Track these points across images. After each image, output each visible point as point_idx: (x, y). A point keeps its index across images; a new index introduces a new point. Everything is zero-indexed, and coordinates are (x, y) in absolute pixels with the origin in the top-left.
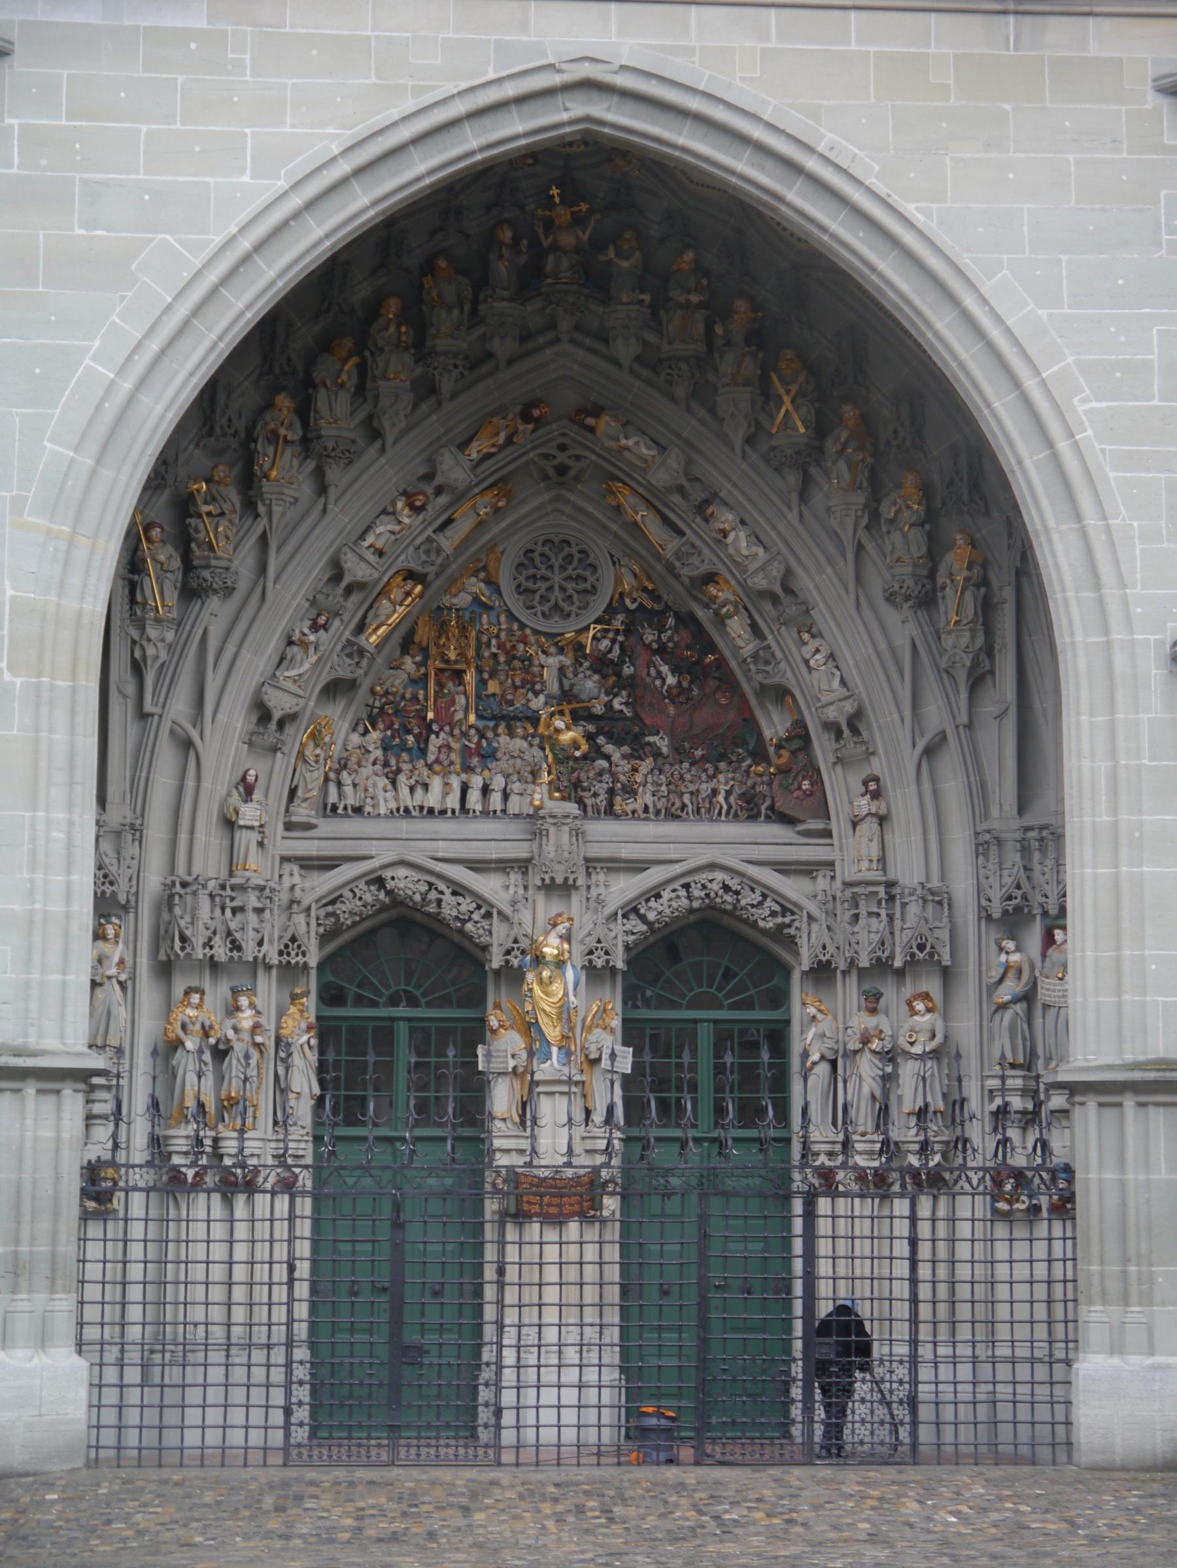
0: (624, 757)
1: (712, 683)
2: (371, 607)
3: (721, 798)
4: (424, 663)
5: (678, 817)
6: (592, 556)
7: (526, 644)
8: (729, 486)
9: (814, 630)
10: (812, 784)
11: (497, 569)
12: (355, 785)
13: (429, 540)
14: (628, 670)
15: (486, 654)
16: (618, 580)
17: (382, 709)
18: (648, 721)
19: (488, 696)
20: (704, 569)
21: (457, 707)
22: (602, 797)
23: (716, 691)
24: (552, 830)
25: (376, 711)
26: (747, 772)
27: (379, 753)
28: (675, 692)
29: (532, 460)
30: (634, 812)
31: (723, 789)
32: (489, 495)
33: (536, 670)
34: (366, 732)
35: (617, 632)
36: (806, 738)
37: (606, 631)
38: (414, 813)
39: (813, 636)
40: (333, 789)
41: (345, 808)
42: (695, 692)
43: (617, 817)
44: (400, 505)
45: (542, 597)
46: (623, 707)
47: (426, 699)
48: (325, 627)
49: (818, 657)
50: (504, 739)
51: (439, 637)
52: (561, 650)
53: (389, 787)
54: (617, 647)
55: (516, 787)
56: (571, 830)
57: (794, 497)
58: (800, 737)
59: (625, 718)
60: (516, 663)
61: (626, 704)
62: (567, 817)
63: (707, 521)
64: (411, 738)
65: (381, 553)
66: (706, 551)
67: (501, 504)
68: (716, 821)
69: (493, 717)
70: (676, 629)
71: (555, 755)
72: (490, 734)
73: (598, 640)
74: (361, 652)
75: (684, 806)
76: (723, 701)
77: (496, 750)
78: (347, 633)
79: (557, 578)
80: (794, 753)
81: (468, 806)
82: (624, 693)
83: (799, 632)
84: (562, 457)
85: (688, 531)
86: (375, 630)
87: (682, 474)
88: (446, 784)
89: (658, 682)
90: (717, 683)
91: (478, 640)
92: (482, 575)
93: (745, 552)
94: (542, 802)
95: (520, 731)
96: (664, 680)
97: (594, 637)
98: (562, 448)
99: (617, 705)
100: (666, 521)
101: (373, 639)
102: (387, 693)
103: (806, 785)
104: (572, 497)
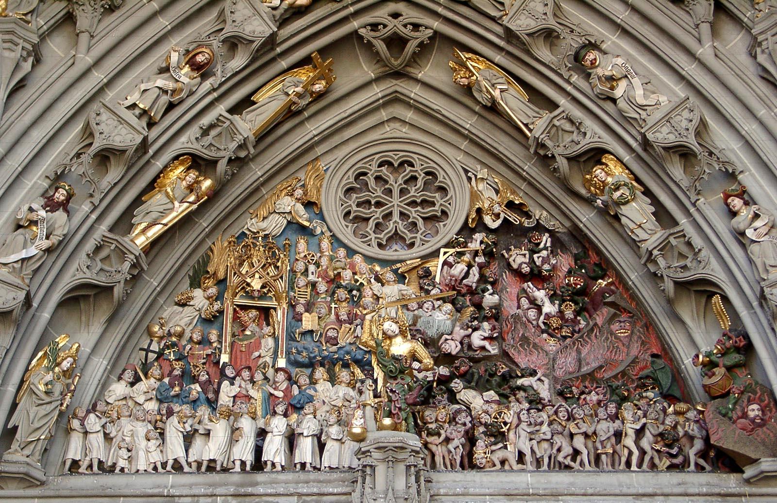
1: (606, 311)
2: (137, 202)
3: (629, 441)
4: (219, 297)
5: (568, 467)
6: (441, 176)
7: (355, 274)
8: (614, 38)
9: (745, 196)
10: (763, 410)
11: (318, 191)
12: (107, 437)
13: (218, 121)
14: (490, 299)
15: (302, 281)
16: (475, 196)
17: (160, 355)
18: (523, 361)
19: (304, 334)
20: (585, 143)
21: (262, 352)
22: (456, 442)
23: (611, 319)
24: (381, 470)
25: (152, 356)
26: (664, 410)
27: (152, 406)
28: (555, 323)
29: (356, 32)
31: (630, 428)
32: (304, 75)
33: (368, 300)
34: (137, 380)
35: (476, 253)
36: (748, 349)
37: (460, 254)
38: (186, 469)
39: (746, 203)
40: (76, 440)
41: (90, 466)
42: (583, 324)
44: (175, 57)
45: (378, 225)
46: (486, 344)
47: (220, 342)
48: (64, 205)
49: (758, 223)
50: (323, 388)
51: (241, 264)
52: (401, 278)
53: (154, 434)
54: (475, 270)
55: (334, 431)
56: (408, 467)
57: (705, 28)
58: (737, 350)
59: (489, 358)
60: (342, 293)
61: (490, 339)
63: (588, 76)
64: (197, 387)
65: (151, 124)
66: (589, 124)
67: (319, 87)
68: (623, 471)
69: (311, 365)
70: (553, 253)
71: (383, 367)
72: (304, 380)
73: (451, 266)
74: (121, 253)
75: (576, 453)
76: (622, 334)
77: (311, 399)
78: (103, 228)
79: (396, 203)
80: (729, 369)
81: (264, 458)
82: (486, 325)
83: (727, 196)
84: (394, 25)
85: (562, 101)
86: (144, 231)
87: (550, 14)
89: (532, 313)
90: (612, 311)
91: (293, 271)
92: (299, 193)
93: (641, 101)
94: (365, 430)
96: (539, 308)
97: (445, 263)
98: (396, 15)
99: (477, 340)
100: (535, 96)
101: (141, 241)
102: (170, 334)
103: (754, 411)
104: (414, 92)
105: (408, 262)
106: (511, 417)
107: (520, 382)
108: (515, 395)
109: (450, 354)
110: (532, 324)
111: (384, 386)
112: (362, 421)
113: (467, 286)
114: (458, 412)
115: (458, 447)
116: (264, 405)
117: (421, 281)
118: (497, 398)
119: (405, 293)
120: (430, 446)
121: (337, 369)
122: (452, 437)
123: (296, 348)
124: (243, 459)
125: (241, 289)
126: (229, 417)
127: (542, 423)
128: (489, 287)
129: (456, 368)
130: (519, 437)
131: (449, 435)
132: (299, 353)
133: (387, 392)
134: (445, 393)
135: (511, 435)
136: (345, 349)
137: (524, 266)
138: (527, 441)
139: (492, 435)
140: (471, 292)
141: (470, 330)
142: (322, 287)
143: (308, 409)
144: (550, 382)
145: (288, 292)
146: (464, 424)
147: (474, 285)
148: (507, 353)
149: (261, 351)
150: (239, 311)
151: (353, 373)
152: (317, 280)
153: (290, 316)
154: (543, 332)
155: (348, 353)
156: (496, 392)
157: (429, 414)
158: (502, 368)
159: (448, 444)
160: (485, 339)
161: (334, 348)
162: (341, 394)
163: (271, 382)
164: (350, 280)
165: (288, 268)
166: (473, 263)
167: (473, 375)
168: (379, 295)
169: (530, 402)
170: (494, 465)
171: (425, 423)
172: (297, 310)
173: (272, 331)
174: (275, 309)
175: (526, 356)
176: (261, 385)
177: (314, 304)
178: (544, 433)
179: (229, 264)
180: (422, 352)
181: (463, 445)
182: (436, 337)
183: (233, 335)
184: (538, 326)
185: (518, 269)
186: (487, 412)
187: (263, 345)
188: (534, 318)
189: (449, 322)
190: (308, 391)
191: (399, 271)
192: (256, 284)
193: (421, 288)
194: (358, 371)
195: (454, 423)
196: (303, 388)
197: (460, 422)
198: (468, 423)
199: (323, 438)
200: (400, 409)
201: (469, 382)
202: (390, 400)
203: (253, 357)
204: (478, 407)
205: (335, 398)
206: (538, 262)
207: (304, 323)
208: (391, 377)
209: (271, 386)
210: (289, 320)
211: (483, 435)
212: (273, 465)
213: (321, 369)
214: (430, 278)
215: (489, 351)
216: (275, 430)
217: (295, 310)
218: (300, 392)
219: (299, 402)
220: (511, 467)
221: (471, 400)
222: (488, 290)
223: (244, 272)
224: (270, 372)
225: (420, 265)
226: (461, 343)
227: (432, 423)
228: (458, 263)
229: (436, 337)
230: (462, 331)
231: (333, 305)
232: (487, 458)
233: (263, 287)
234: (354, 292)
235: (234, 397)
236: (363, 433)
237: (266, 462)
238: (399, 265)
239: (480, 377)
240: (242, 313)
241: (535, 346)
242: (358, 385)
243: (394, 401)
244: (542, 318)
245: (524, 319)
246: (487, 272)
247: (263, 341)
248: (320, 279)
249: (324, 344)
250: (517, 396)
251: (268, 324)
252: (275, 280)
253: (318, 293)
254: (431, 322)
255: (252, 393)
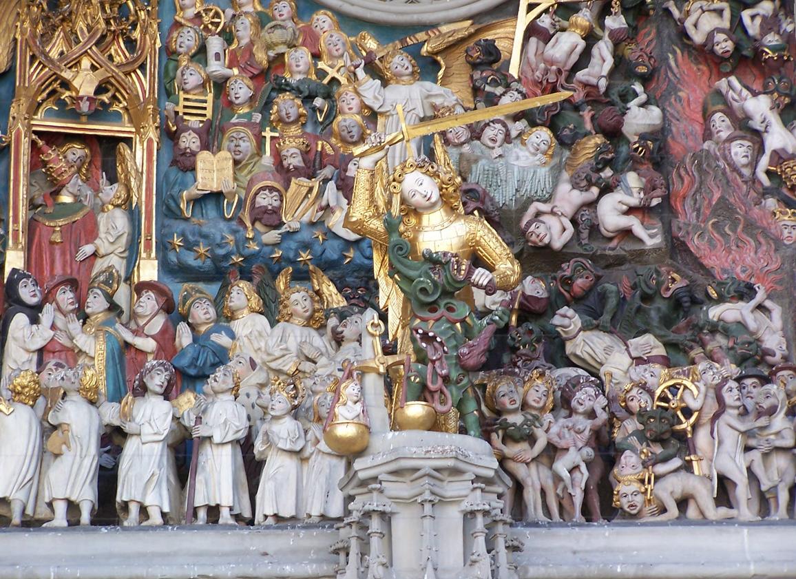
0: (639, 361)
7: (317, 56)
15: (193, 77)
19: (199, 201)
21: (103, 244)
30: (683, 503)
33: (349, 118)
43: (631, 518)
46: (634, 223)
51: (46, 37)
52: (427, 67)
54: (604, 50)
56: (469, 516)
59: (640, 256)
60: (287, 104)
62: (456, 472)
72: (203, 312)
73: (546, 37)
81: (122, 495)
82: (632, 179)
88: (48, 429)
89: (740, 151)
91: (169, 53)
95: (298, 299)
96: (757, 137)
97: (532, 30)
99: (611, 212)
105: (444, 29)
106: (702, 396)
107: (714, 313)
108: (703, 345)
109: (548, 247)
110: (741, 175)
111: (405, 323)
112: (358, 407)
113: (586, 85)
114: (575, 384)
115: (577, 467)
116: (111, 371)
117: (477, 75)
118: (660, 351)
119: (438, 101)
120: (511, 465)
121: (281, 283)
122: (562, 444)
123: (183, 235)
124: (73, 498)
125: (49, 95)
126: (35, 399)
127: (772, 411)
128: (638, 87)
129: (567, 282)
130: (720, 443)
131: (555, 440)
132: (189, 246)
133: (413, 340)
134: (538, 341)
135: (702, 439)
136: (299, 237)
137: (720, 37)
138: (740, 449)
139: (660, 440)
140: (593, 97)
141: (595, 191)
142: (241, 90)
143: (220, 379)
144: (783, 313)
145: (158, 103)
146: (592, 414)
147: (603, 83)
148: (684, 244)
149: (97, 241)
150: (45, 148)
151: (318, 293)
152: (227, 72)
153: (167, 158)
154: (766, 192)
155: (306, 246)
156: (657, 336)
157: (506, 390)
158: (674, 280)
159: (552, 460)
160: (631, 211)
161: (272, 236)
162: (292, 344)
163: (125, 317)
164: (307, 73)
165: (158, 44)
166: (598, 31)
167: (603, 297)
168: (376, 107)
169: (741, 361)
170: (664, 510)
171: (499, 413)
172: (182, 145)
173: (123, 195)
174: (128, 141)
175: (729, 251)
176: (105, 323)
177: (223, 131)
178: (778, 433)
179: (19, 37)
180: (493, 244)
181: (589, 465)
182: (513, 206)
183: (32, 205)
184: (754, 179)
185: (704, 45)
186: (644, 387)
187: (102, 228)
188: (745, 161)
189: (543, 172)
190: (214, 337)
191: (425, 50)
192: (85, 83)
193: (476, 91)
194: (329, 290)
195: (564, 412)
196: (203, 329)
197: (581, 409)
198: (599, 411)
199: (259, 447)
200: (446, 379)
201: (596, 314)
202: (422, 359)
203: (80, 257)
204: (618, 375)
205: (277, 354)
206: (753, 28)
207: (200, 175)
208: (424, 305)
209: (126, 325)
210: (165, 168)
211: (634, 440)
212: (143, 511)
213: (242, 284)
214: (495, 66)
215: (640, 241)
216: (146, 430)
217: (177, 144)
218: (195, 340)
219: (193, 363)
220: (702, 513)
221: (601, 356)
222: (636, 95)
223: (54, 54)
224: (122, 295)
225: (471, 36)
226: (574, 221)
227: (514, 411)
228: (563, 30)
229: (513, 206)
230: (576, 193)
231: (268, 134)
232: (645, 493)
233: (100, 90)
234: (318, 102)
235: (41, 351)
236: (361, 436)
237: (125, 506)
238: (421, 36)
239: (622, 301)
240: (51, 154)
241: (750, 227)
242: (333, 322)
243: (433, 362)
244: (764, 162)
245: (722, 163)
246: (630, 52)
247: (102, 219)
248: (236, 71)
249: (249, 224)
250: (709, 347)
251: (113, 179)
252: (128, 74)
253: (231, 103)
254: (502, 170)
255: (84, 341)
